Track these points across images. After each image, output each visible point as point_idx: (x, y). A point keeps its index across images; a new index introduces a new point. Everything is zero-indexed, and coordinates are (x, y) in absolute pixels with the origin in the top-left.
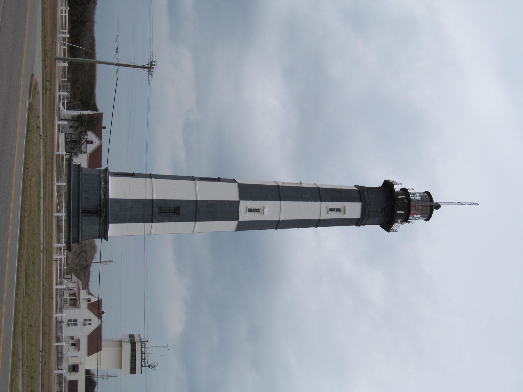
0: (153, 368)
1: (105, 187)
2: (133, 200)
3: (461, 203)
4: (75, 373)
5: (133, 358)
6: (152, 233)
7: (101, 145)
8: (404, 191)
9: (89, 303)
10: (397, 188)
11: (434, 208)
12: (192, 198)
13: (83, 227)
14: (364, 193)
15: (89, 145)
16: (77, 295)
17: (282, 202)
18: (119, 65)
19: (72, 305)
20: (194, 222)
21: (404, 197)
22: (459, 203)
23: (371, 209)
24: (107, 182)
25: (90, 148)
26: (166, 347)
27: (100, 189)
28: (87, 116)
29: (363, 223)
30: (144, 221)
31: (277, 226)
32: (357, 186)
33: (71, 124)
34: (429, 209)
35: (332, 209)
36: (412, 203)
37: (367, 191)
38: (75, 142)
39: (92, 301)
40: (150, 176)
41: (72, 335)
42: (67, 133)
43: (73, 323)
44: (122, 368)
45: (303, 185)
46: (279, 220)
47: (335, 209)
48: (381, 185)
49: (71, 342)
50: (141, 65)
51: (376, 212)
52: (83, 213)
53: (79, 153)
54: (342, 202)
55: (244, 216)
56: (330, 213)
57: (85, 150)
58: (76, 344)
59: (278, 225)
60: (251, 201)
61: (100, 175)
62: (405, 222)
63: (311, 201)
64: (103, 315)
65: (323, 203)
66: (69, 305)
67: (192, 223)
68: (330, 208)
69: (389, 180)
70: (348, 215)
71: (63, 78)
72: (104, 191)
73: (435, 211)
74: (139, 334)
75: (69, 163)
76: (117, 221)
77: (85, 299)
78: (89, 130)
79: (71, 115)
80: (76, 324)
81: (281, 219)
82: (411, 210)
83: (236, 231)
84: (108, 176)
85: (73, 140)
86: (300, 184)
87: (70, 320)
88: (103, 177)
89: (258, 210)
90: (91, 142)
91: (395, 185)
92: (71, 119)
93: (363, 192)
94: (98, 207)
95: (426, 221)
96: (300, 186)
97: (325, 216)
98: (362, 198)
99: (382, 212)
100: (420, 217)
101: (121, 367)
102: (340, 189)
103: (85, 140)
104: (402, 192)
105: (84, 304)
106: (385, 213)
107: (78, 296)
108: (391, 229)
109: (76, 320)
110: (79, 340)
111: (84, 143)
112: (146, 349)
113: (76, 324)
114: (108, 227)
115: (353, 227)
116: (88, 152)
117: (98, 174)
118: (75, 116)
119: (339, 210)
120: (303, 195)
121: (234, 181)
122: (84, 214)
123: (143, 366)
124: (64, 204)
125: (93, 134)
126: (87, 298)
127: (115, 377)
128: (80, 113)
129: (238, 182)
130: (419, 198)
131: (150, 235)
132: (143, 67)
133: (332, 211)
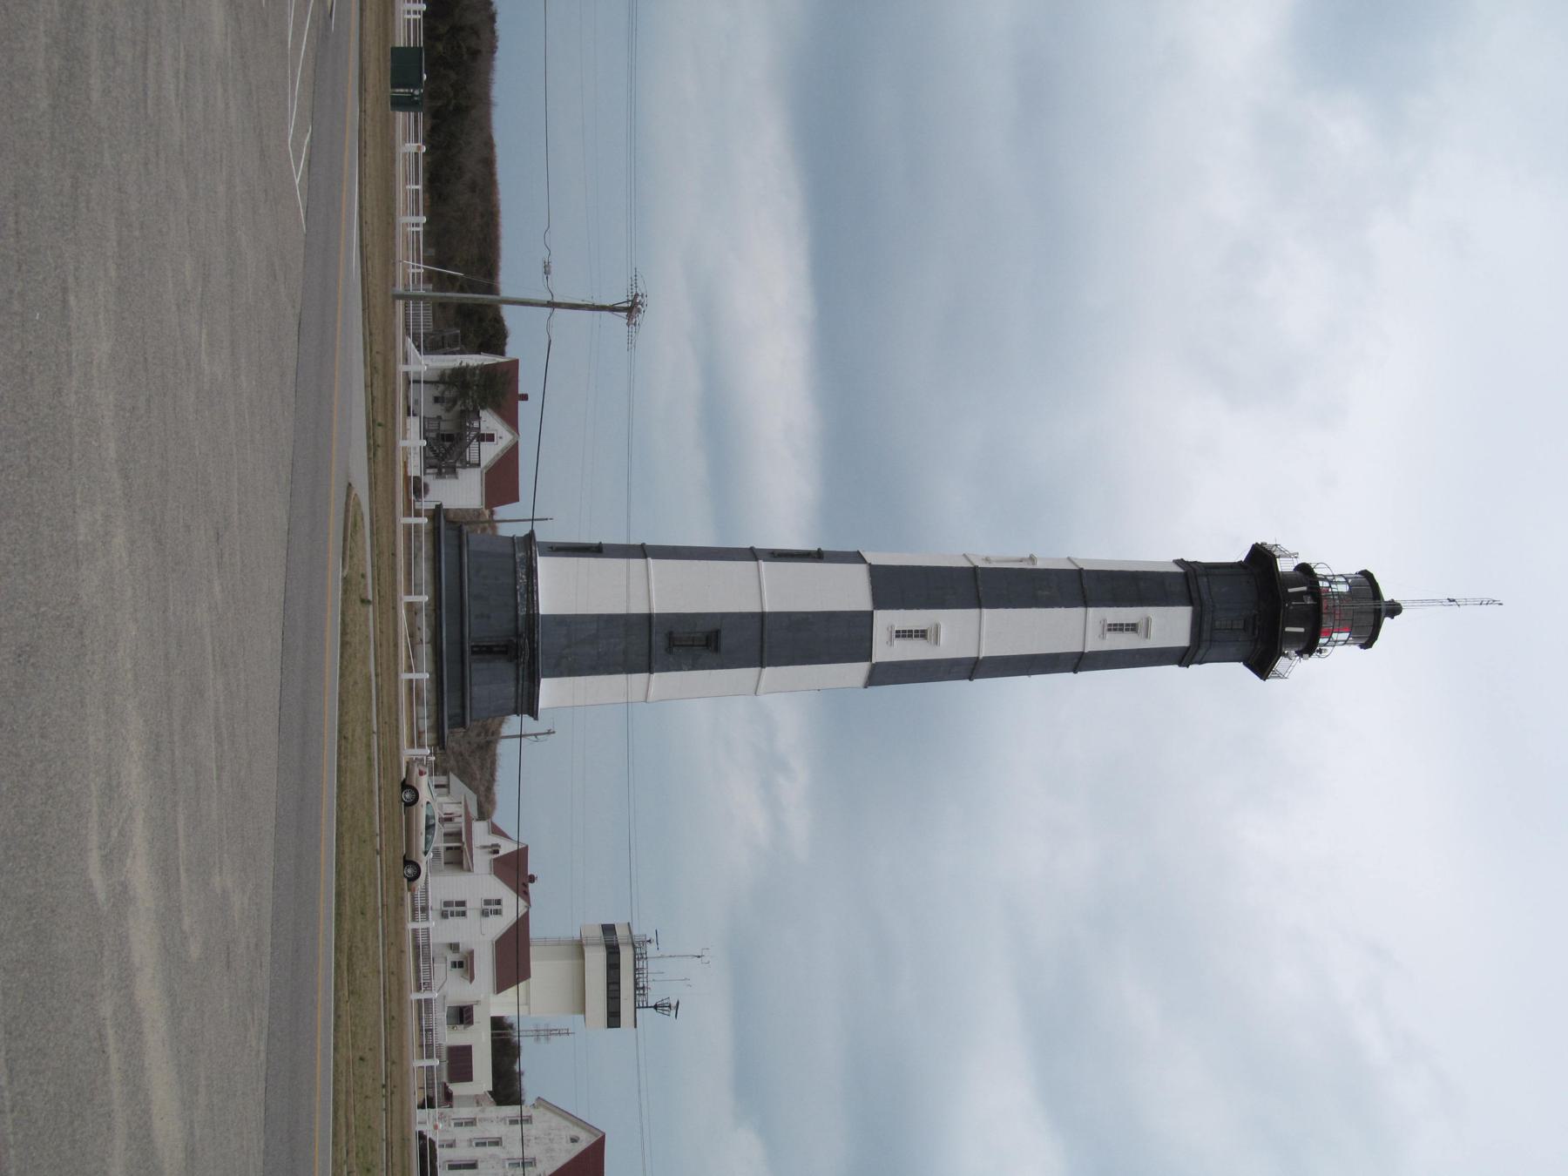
0: (665, 1012)
1: (527, 586)
2: (599, 617)
3: (1454, 601)
4: (465, 1028)
5: (612, 987)
6: (651, 698)
7: (517, 442)
8: (1305, 570)
9: (496, 856)
10: (1285, 566)
11: (1383, 614)
12: (752, 607)
13: (475, 689)
14: (1197, 583)
15: (484, 445)
16: (464, 839)
17: (985, 611)
18: (552, 305)
19: (451, 863)
20: (757, 669)
21: (1304, 588)
22: (1450, 600)
23: (1217, 623)
24: (532, 572)
25: (489, 453)
26: (699, 957)
27: (516, 591)
28: (477, 372)
29: (1198, 658)
30: (630, 669)
31: (974, 669)
32: (1180, 562)
33: (437, 393)
34: (1371, 619)
35: (1115, 625)
36: (1324, 605)
37: (1207, 575)
38: (450, 437)
39: (502, 852)
40: (643, 551)
41: (453, 941)
42: (427, 416)
43: (455, 909)
44: (585, 1014)
45: (1040, 565)
46: (978, 658)
47: (1122, 625)
48: (1243, 558)
49: (452, 957)
50: (608, 303)
51: (1231, 629)
52: (473, 653)
53: (459, 467)
54: (1142, 605)
55: (885, 650)
56: (1109, 635)
57: (474, 459)
58: (465, 962)
59: (974, 668)
60: (902, 612)
61: (515, 555)
62: (1308, 655)
63: (1060, 607)
64: (530, 885)
65: (1091, 610)
66: (445, 863)
67: (754, 671)
68: (1108, 622)
69: (1266, 544)
70: (1156, 641)
72: (526, 596)
73: (1387, 621)
74: (629, 924)
75: (434, 529)
76: (559, 671)
77: (485, 847)
78: (483, 408)
79: (437, 369)
80: (463, 914)
81: (982, 655)
82: (1324, 621)
83: (866, 687)
84: (534, 555)
85: (443, 435)
86: (1030, 563)
87: (447, 904)
88: (521, 559)
89: (922, 634)
90: (491, 438)
91: (1279, 557)
92: (436, 379)
93: (1196, 579)
94: (512, 638)
95: (1365, 649)
96: (1030, 566)
97: (1094, 644)
98: (1194, 595)
99: (1245, 629)
100: (1346, 639)
101: (583, 1011)
102: (1137, 571)
103: (473, 434)
104: (1298, 573)
105: (482, 861)
106: (1254, 634)
107: (467, 839)
108: (1271, 670)
109: (462, 904)
110: (471, 953)
111: (472, 441)
112: (645, 962)
113: (463, 914)
114: (537, 688)
115: (1174, 669)
116: (483, 464)
117: (509, 550)
118: (448, 372)
119: (1133, 628)
120: (1039, 592)
121: (857, 558)
122: (475, 657)
123: (639, 1007)
124: (425, 634)
125: (496, 417)
126: (490, 844)
127: (568, 1034)
128: (461, 364)
129: (869, 562)
130: (1344, 588)
131: (646, 701)
132: (613, 309)
133: (1115, 630)
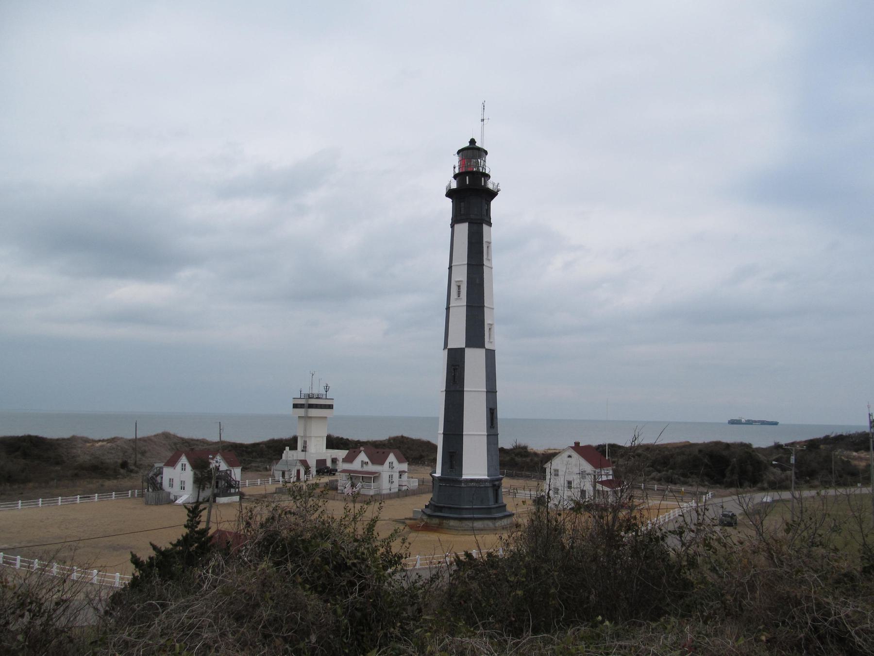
71: (112, 497)
98: (479, 221)
101: (326, 417)
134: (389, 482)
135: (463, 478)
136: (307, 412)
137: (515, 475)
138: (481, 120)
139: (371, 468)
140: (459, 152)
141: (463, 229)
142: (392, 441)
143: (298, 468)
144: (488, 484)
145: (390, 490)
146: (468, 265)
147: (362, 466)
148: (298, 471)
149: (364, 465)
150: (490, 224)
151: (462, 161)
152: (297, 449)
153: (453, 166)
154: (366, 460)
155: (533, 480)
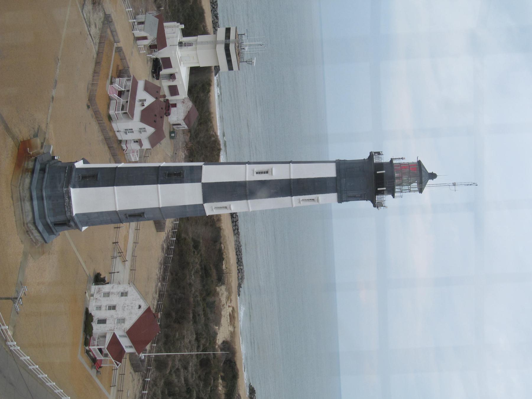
2: (97, 213)
9: (144, 107)
43: (129, 131)
54: (315, 194)
88: (66, 191)
134: (125, 130)
135: (71, 188)
136: (221, 42)
137: (166, 266)
138: (455, 183)
139: (138, 109)
140: (419, 162)
141: (330, 171)
142: (213, 139)
143: (149, 38)
144: (68, 214)
145: (118, 131)
146: (290, 181)
147: (140, 101)
148: (145, 38)
149: (141, 103)
150: (340, 200)
151: (408, 166)
152: (183, 37)
153: (403, 157)
154: (146, 104)
155: (159, 284)
